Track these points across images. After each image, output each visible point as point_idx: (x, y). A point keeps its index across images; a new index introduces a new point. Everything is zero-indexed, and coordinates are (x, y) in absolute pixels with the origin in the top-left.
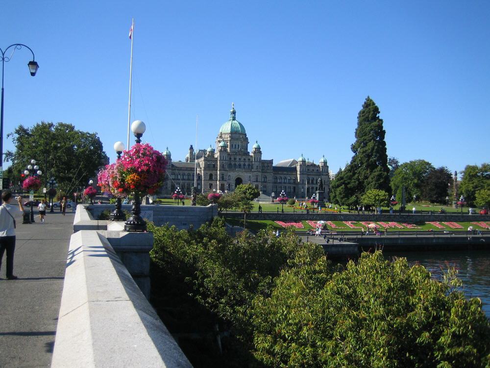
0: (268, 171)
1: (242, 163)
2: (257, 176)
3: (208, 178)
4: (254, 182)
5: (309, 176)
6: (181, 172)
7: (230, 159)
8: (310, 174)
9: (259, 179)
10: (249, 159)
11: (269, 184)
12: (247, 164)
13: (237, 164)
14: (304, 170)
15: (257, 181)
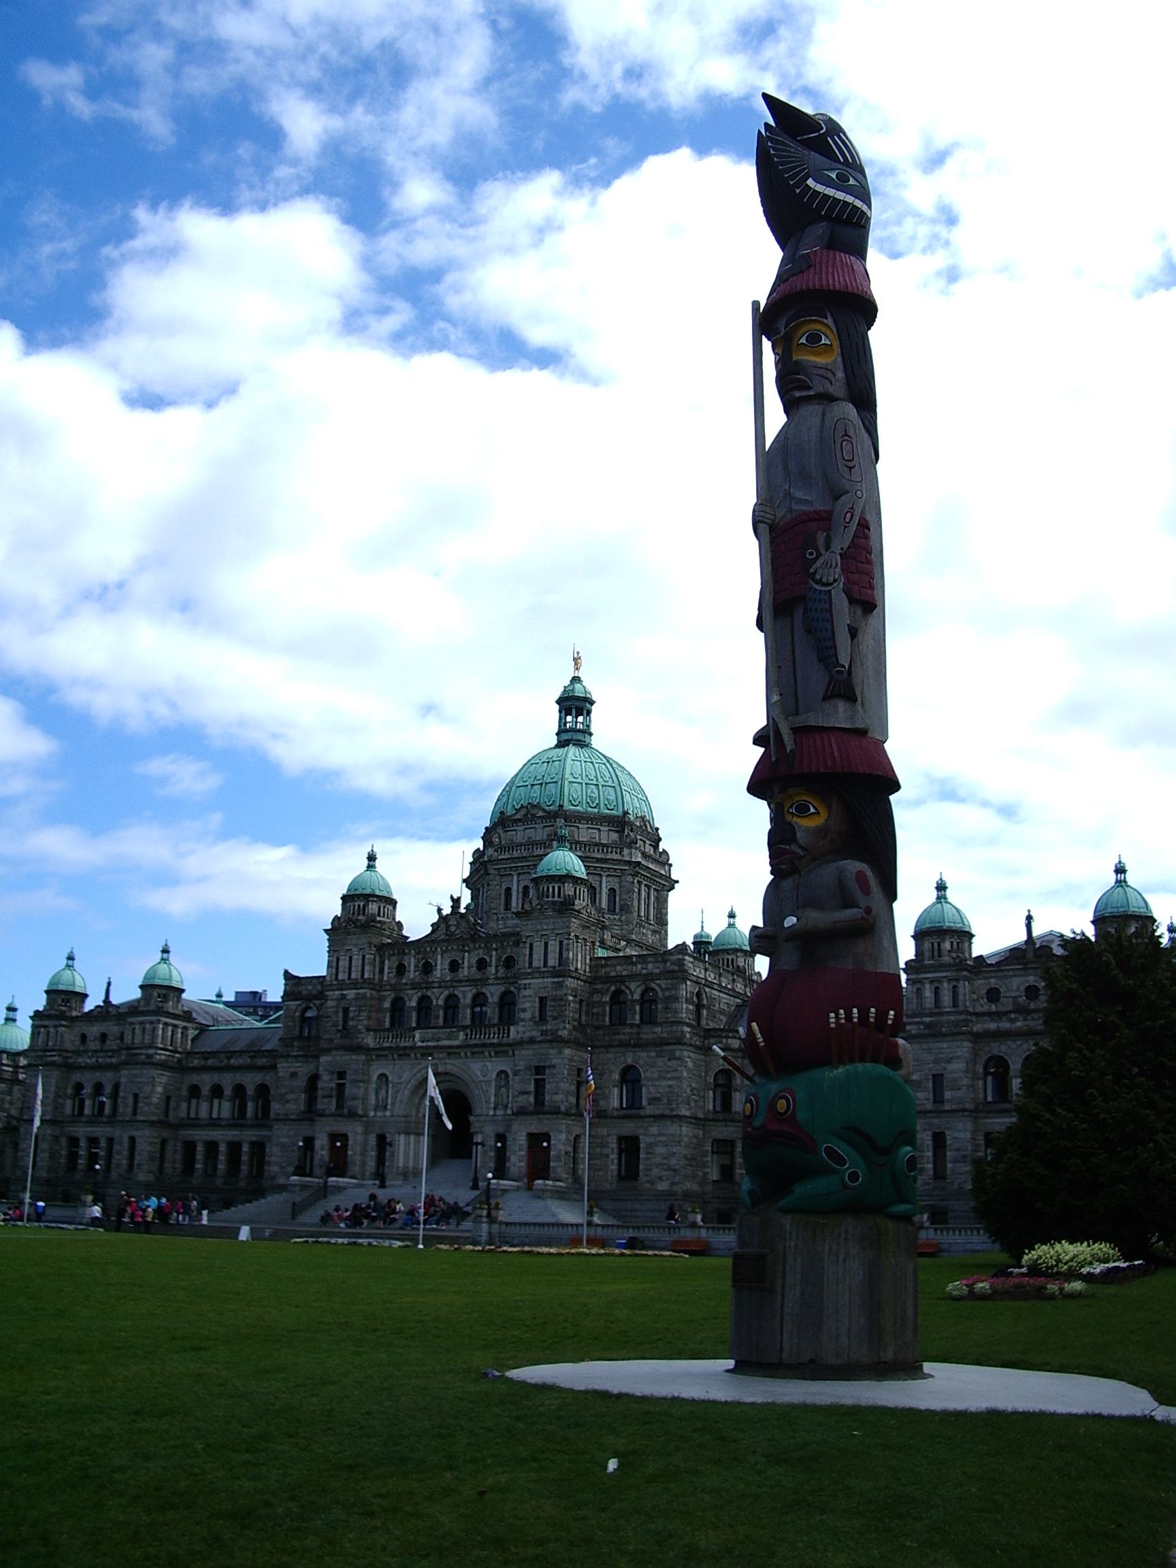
0: (649, 1033)
1: (466, 995)
2: (539, 1070)
3: (297, 1104)
4: (521, 1112)
5: (998, 1048)
6: (227, 1082)
7: (401, 970)
8: (1005, 1025)
9: (560, 1092)
10: (509, 962)
11: (654, 1130)
12: (493, 993)
13: (439, 998)
14: (946, 999)
15: (540, 1107)
